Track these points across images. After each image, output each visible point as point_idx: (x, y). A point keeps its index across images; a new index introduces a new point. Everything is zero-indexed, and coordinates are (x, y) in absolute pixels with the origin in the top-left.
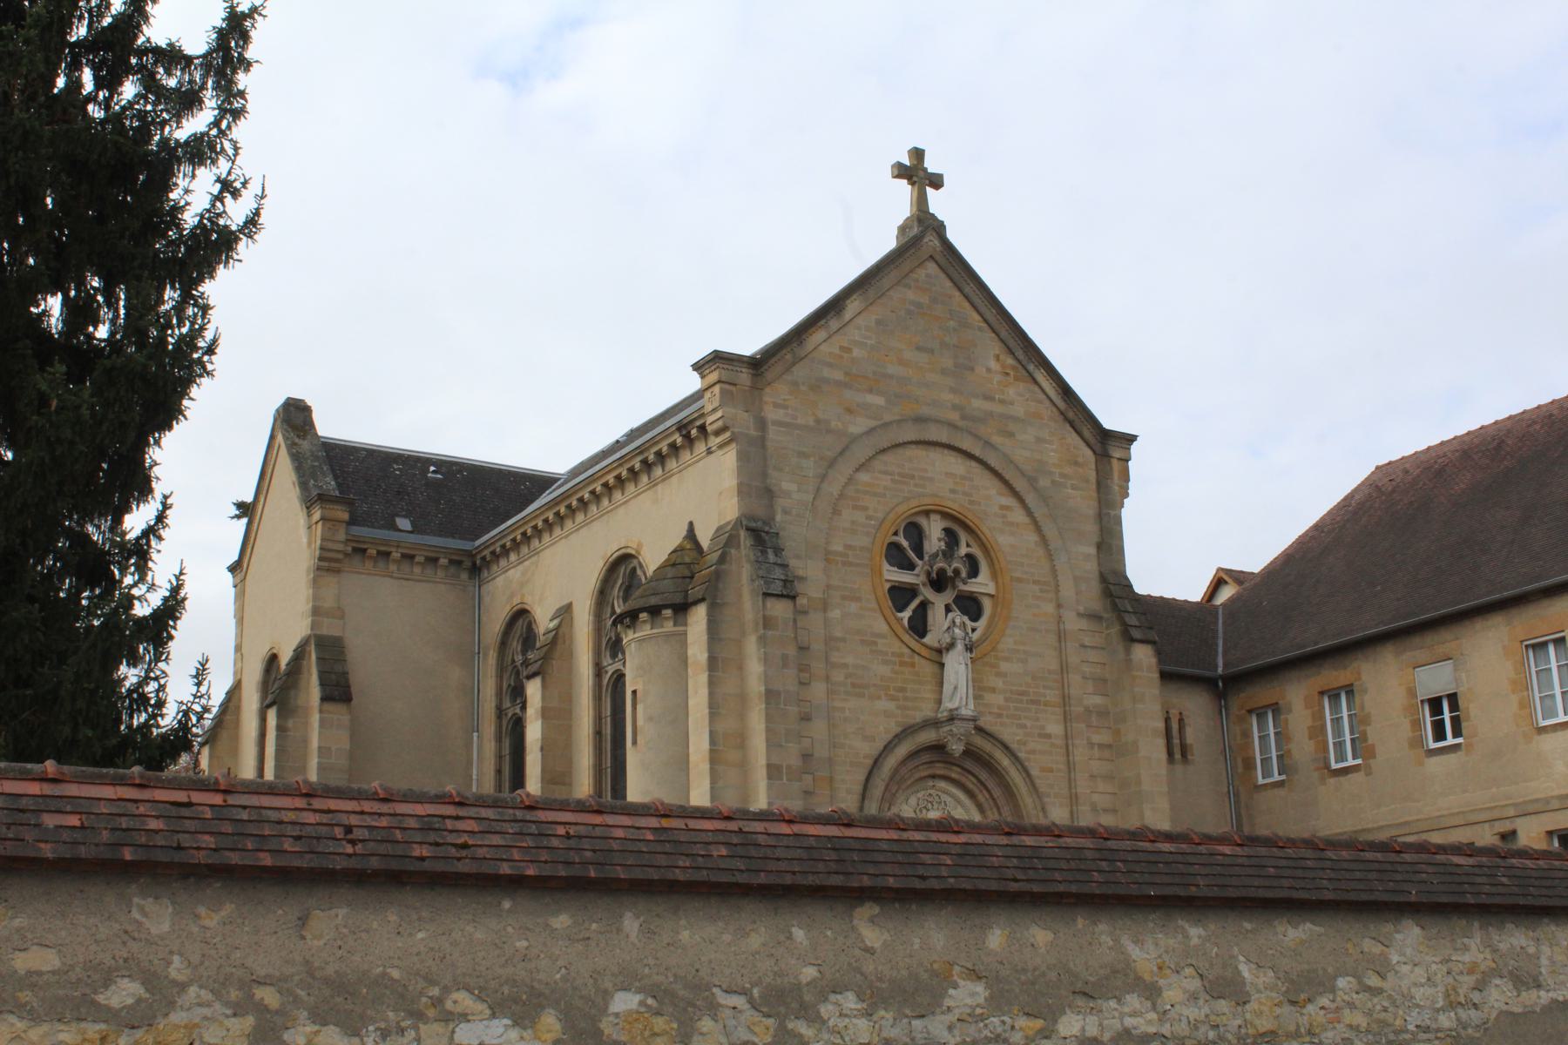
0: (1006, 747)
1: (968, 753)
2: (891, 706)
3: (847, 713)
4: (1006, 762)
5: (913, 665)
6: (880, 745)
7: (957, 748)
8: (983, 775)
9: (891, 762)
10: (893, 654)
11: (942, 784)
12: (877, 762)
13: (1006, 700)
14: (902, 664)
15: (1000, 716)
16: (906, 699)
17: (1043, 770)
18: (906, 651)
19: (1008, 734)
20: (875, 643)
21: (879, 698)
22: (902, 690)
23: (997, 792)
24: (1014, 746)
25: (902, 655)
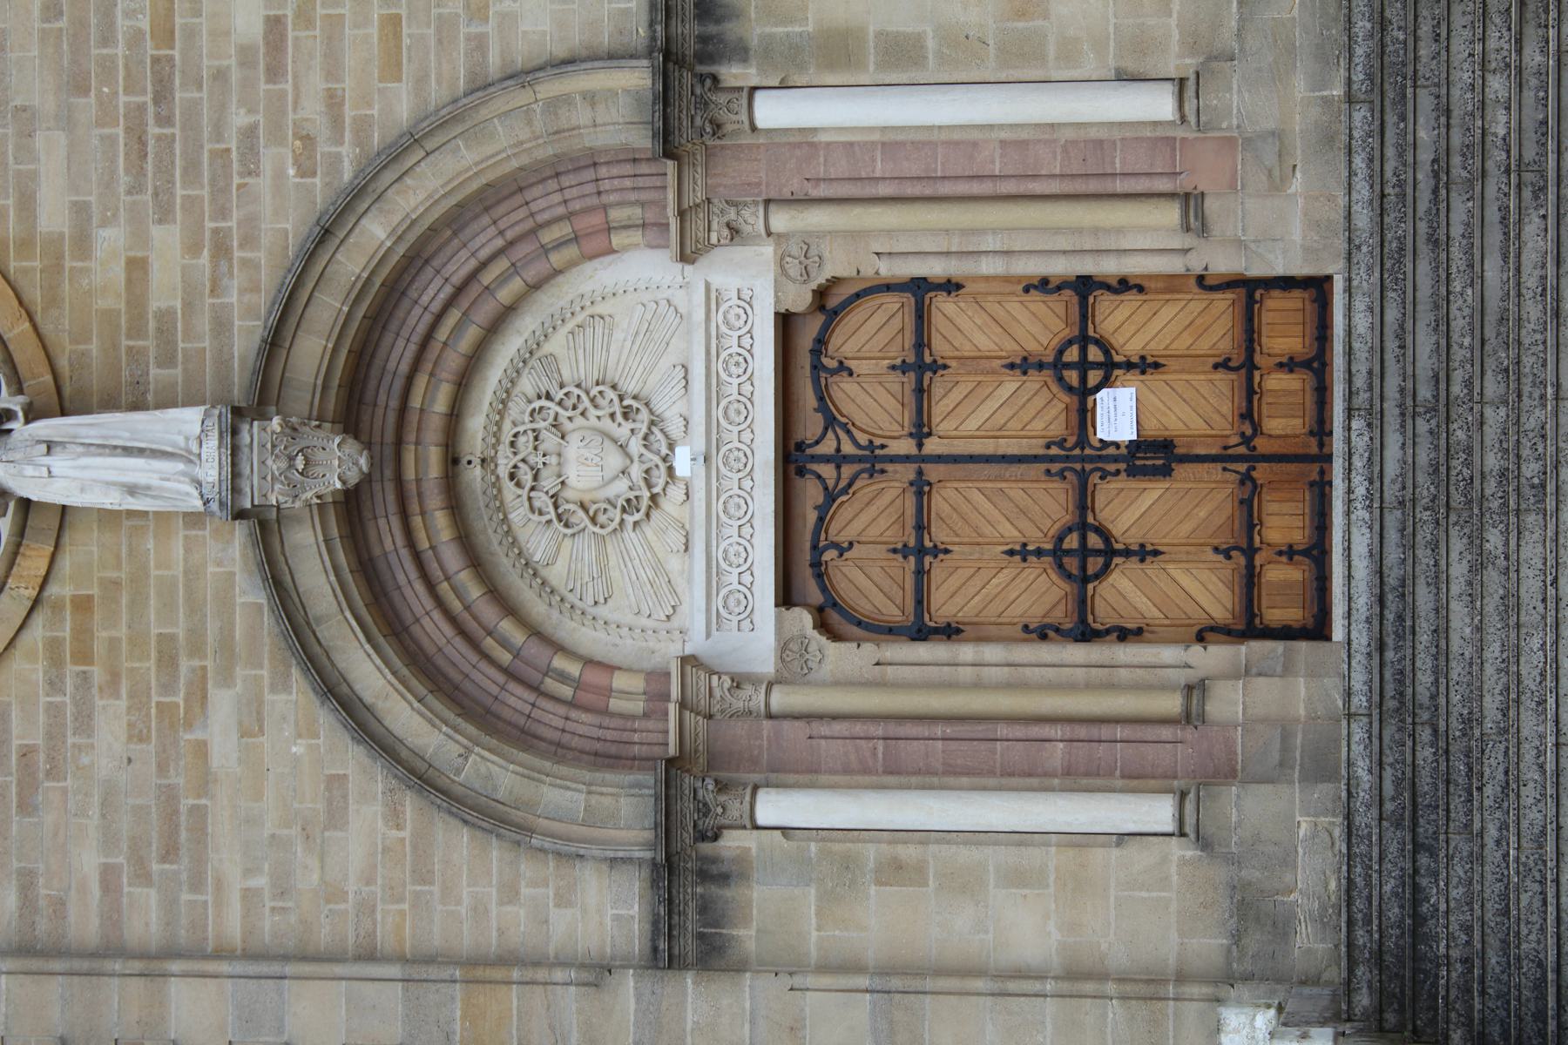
0: (326, 233)
1: (350, 416)
2: (223, 704)
3: (261, 881)
4: (376, 232)
5: (83, 605)
6: (353, 759)
7: (339, 463)
8: (431, 291)
9: (405, 716)
10: (54, 685)
11: (476, 425)
12: (418, 776)
13: (165, 215)
14: (83, 655)
15: (221, 249)
16: (196, 649)
17: (392, 68)
18: (38, 631)
19: (279, 213)
20: (26, 753)
21: (201, 749)
22: (168, 661)
23: (485, 240)
24: (320, 192)
25: (54, 646)
